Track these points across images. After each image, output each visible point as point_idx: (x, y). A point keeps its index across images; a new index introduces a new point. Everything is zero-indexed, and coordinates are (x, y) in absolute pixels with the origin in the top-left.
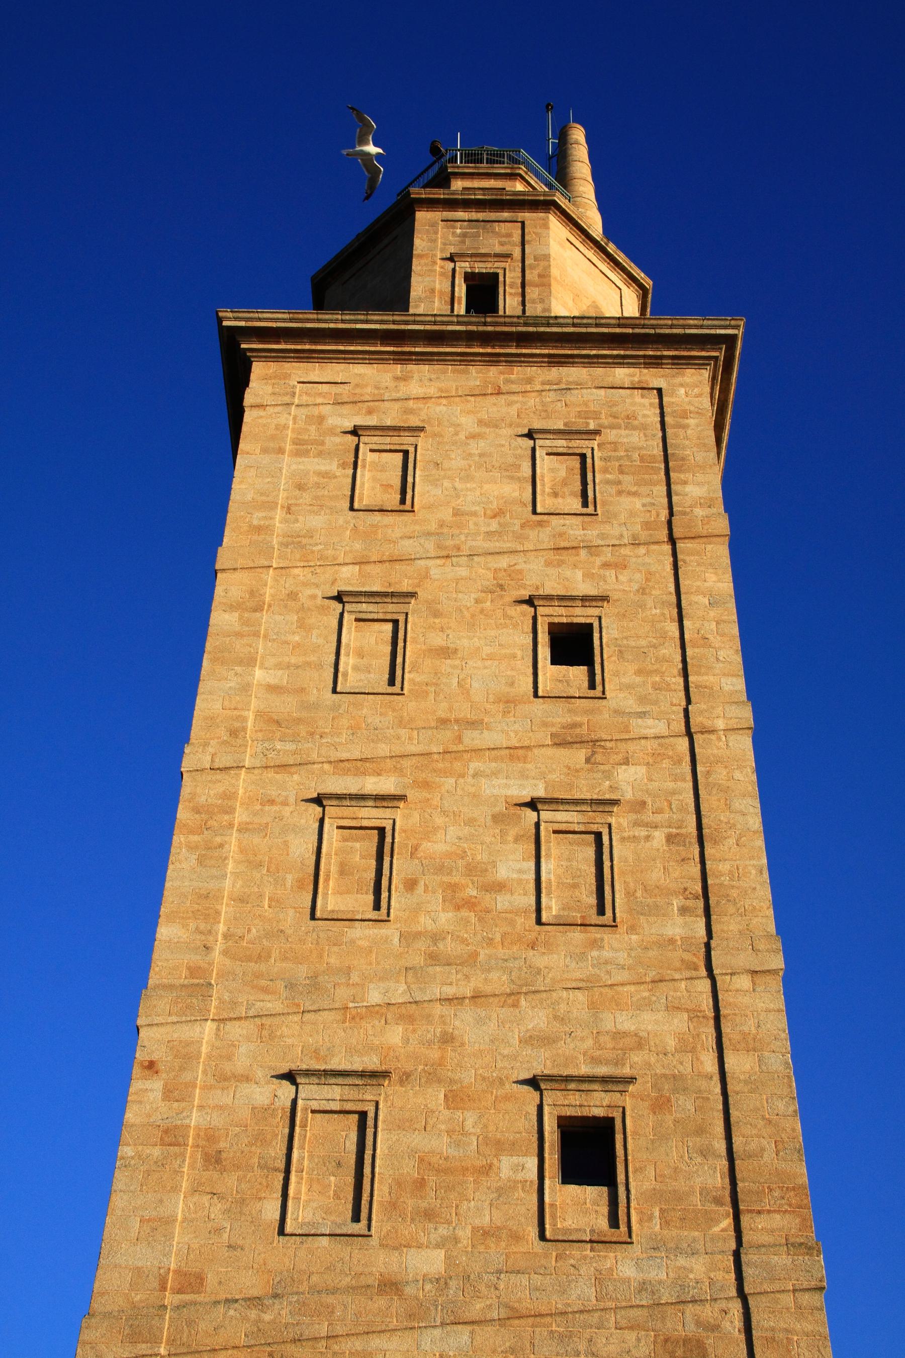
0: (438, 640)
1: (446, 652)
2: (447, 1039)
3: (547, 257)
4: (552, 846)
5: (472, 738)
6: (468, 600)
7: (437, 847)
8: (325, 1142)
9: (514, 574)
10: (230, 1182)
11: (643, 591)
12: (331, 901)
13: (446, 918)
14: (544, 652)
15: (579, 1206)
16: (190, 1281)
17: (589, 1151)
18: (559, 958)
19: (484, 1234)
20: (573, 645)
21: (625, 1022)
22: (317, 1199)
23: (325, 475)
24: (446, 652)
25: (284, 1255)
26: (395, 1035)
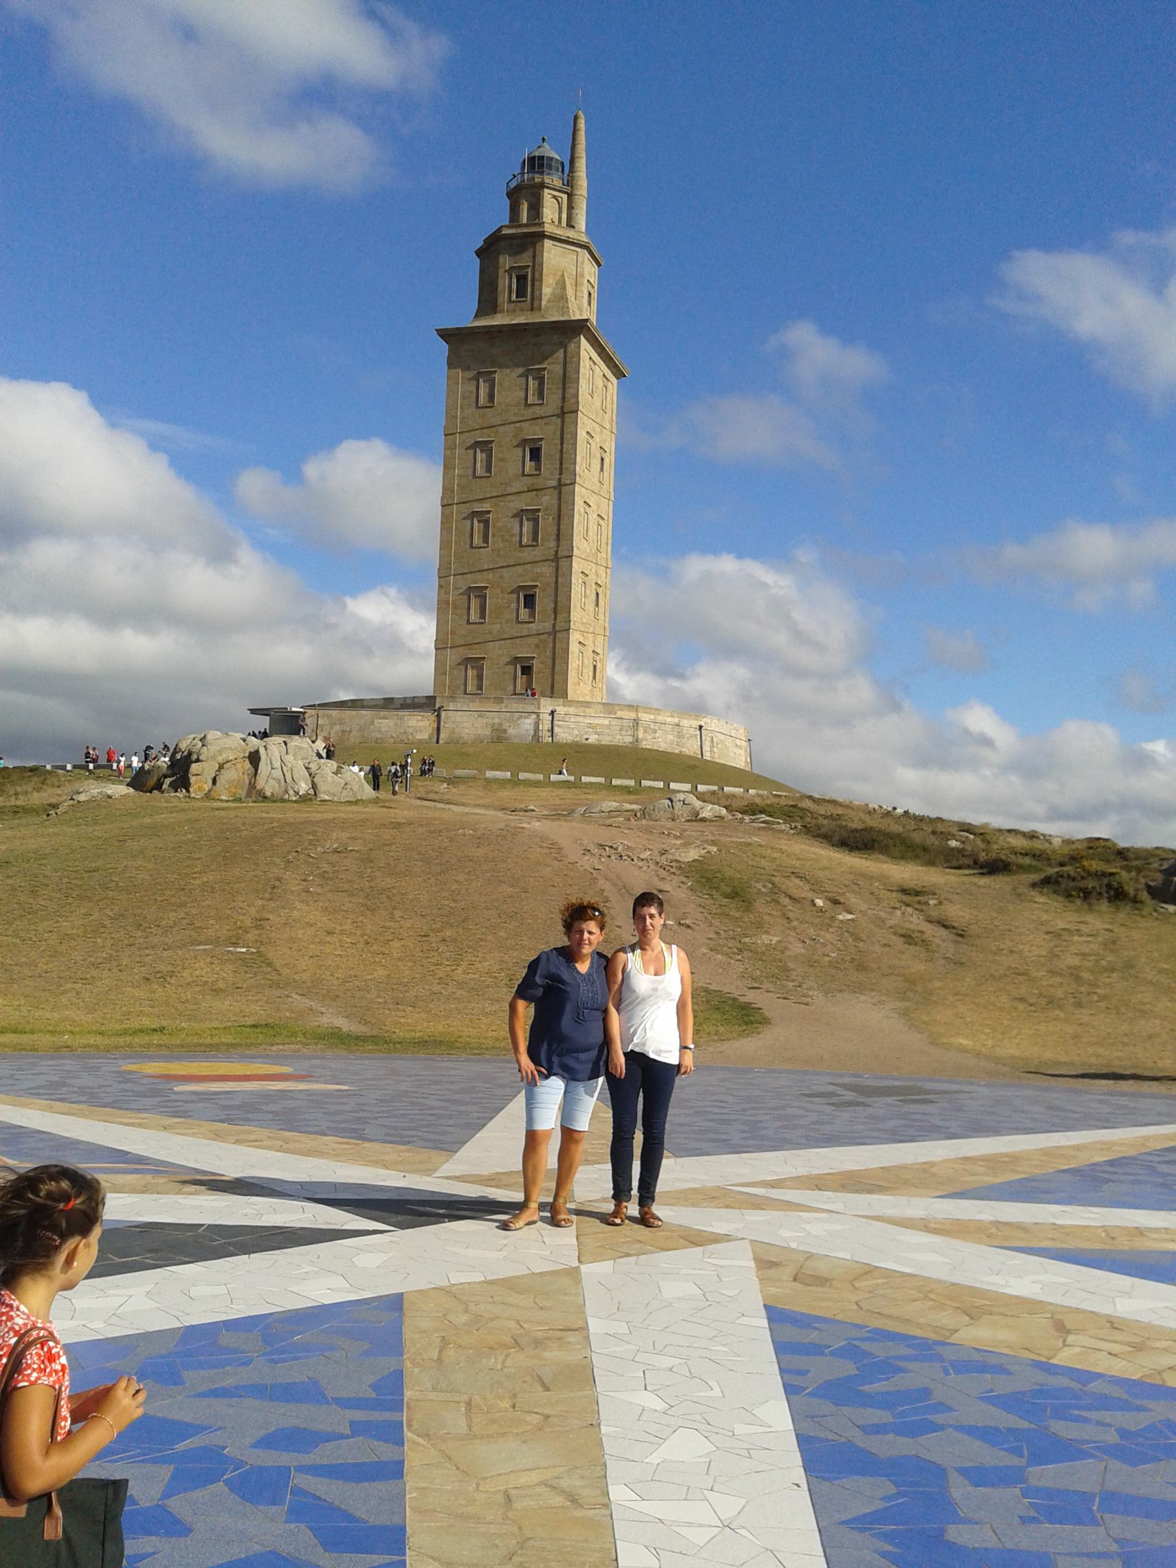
0: (501, 455)
1: (502, 460)
2: (502, 577)
3: (542, 264)
4: (526, 523)
5: (510, 490)
6: (508, 439)
7: (499, 524)
8: (474, 603)
9: (521, 429)
10: (459, 612)
11: (554, 434)
12: (476, 541)
13: (501, 545)
14: (528, 458)
15: (524, 613)
16: (453, 633)
17: (530, 601)
18: (527, 555)
19: (508, 621)
20: (536, 454)
21: (539, 570)
22: (474, 617)
23: (470, 392)
24: (502, 460)
25: (470, 626)
26: (491, 576)
